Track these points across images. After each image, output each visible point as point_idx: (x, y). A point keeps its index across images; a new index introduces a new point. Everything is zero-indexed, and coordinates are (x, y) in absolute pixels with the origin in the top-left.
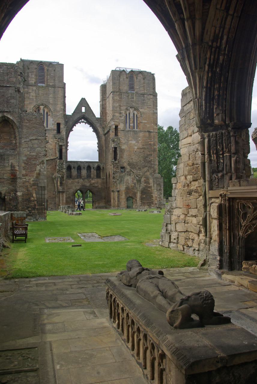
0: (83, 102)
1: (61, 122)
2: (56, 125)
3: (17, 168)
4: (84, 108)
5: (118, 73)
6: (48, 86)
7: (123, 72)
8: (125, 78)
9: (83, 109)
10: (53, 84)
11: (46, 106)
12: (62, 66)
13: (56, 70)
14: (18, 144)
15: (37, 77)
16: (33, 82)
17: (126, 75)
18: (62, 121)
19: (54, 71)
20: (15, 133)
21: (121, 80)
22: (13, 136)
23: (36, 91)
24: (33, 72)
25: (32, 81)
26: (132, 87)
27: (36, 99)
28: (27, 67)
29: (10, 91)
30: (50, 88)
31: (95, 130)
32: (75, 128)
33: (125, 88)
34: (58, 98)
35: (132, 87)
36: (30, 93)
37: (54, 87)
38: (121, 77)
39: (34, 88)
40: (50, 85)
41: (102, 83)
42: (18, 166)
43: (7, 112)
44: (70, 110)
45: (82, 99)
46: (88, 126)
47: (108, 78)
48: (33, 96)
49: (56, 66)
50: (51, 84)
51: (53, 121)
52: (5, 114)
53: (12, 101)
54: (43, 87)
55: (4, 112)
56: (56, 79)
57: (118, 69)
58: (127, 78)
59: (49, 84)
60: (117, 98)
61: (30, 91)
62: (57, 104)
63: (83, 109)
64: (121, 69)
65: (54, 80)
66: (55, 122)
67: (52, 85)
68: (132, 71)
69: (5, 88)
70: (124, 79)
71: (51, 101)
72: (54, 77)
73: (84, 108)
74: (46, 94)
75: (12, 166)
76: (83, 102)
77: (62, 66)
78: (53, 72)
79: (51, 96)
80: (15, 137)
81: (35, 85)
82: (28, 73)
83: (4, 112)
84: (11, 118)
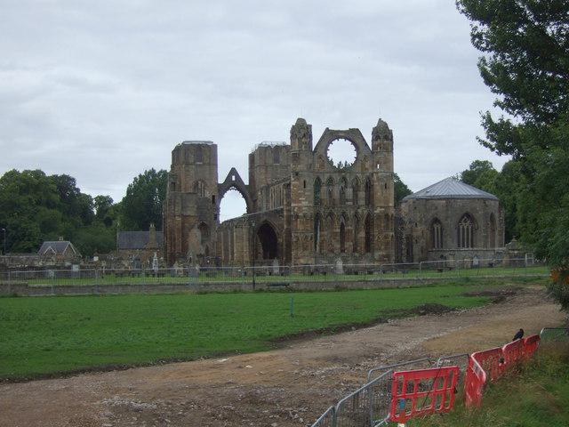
0: (233, 171)
6: (204, 164)
9: (234, 178)
11: (203, 181)
12: (216, 145)
26: (276, 160)
31: (244, 196)
32: (226, 195)
33: (270, 161)
35: (276, 160)
37: (209, 164)
44: (221, 180)
46: (237, 192)
60: (263, 171)
63: (234, 178)
68: (277, 147)
76: (233, 171)
77: (216, 145)
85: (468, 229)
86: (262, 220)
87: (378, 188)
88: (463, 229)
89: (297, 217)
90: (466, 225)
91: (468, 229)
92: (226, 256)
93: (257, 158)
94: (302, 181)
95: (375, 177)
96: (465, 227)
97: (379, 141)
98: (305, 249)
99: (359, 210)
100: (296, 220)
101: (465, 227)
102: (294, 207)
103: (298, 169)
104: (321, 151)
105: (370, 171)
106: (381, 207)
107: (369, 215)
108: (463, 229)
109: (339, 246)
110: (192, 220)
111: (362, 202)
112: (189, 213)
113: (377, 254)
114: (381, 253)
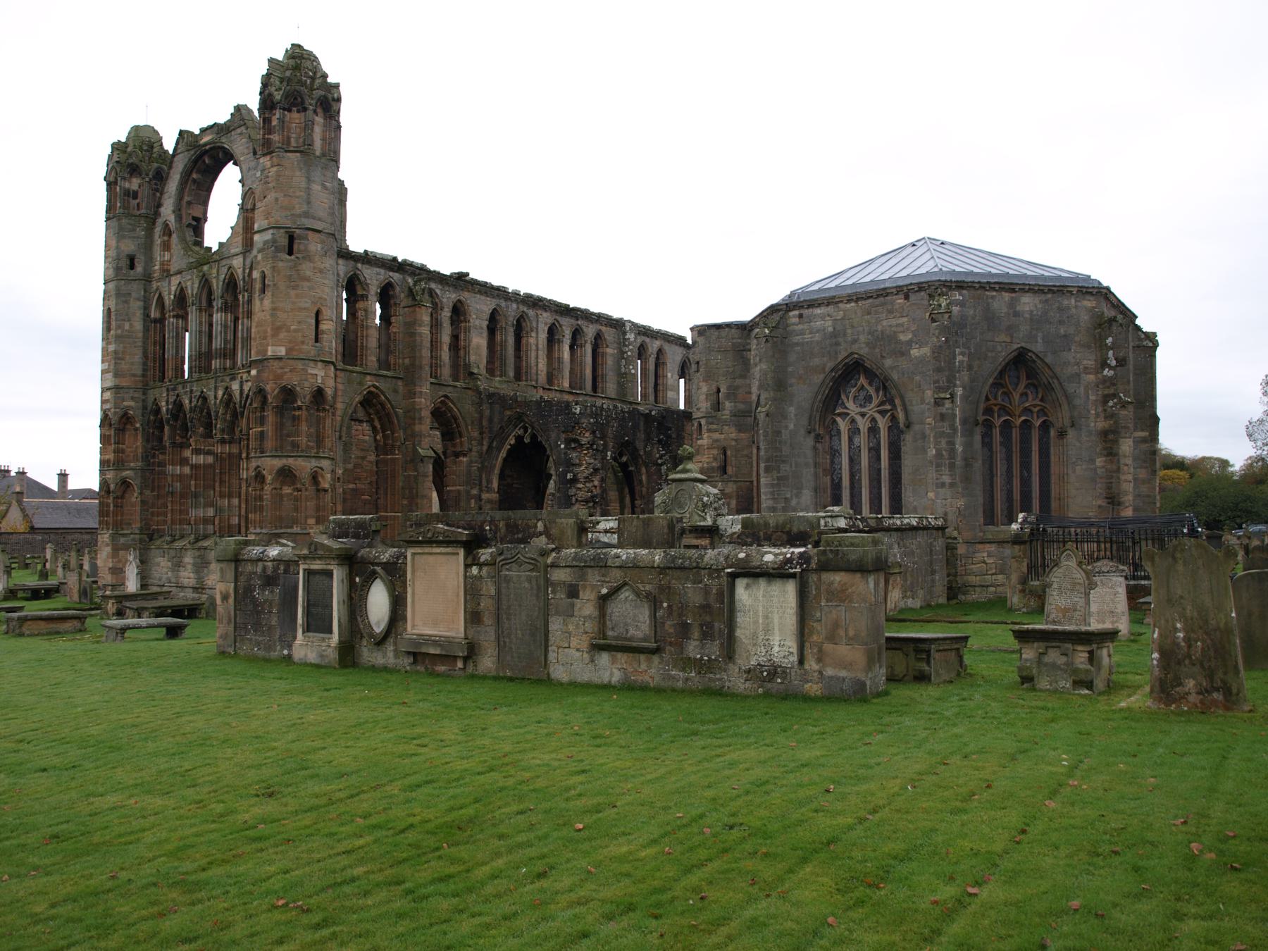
85: (873, 430)
91: (873, 430)
96: (863, 424)
99: (235, 386)
101: (863, 424)
108: (854, 431)
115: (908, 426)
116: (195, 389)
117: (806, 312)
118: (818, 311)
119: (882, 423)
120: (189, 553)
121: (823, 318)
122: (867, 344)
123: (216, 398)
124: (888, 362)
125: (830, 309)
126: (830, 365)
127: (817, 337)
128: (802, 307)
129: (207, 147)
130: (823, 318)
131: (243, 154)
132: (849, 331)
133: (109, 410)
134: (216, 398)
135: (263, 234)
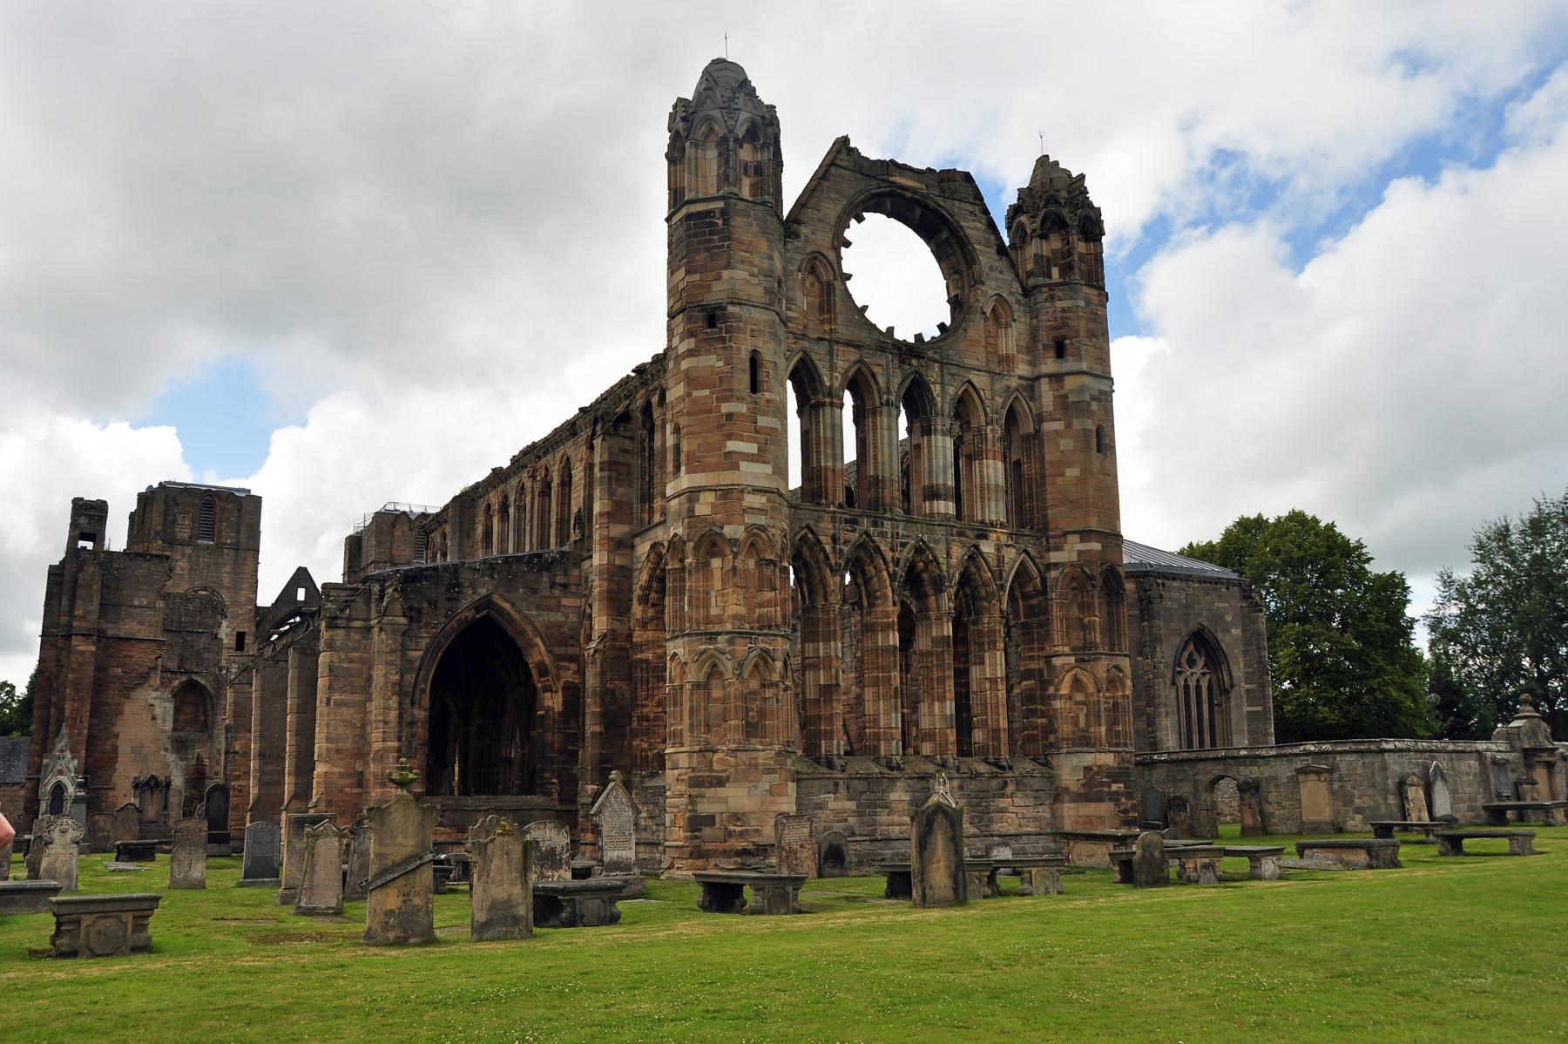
1: (247, 630)
2: (235, 638)
3: (207, 762)
4: (303, 590)
5: (391, 519)
6: (220, 547)
7: (404, 517)
8: (406, 529)
9: (301, 594)
10: (234, 541)
12: (258, 500)
13: (243, 510)
14: (210, 723)
15: (197, 525)
16: (186, 536)
17: (410, 523)
18: (248, 628)
19: (239, 510)
20: (205, 705)
21: (397, 533)
22: (201, 709)
23: (190, 557)
24: (187, 513)
25: (183, 533)
27: (190, 574)
28: (174, 501)
29: (203, 639)
30: (226, 551)
34: (244, 573)
36: (177, 561)
38: (397, 526)
39: (188, 550)
40: (225, 544)
41: (351, 532)
42: (209, 758)
43: (196, 673)
45: (300, 569)
47: (367, 523)
48: (182, 569)
49: (244, 501)
50: (229, 541)
51: (228, 627)
52: (194, 677)
53: (206, 655)
54: (208, 547)
55: (192, 672)
56: (243, 529)
57: (391, 507)
58: (411, 530)
59: (223, 540)
61: (178, 558)
62: (242, 589)
63: (301, 594)
64: (398, 508)
65: (238, 532)
66: (233, 630)
67: (231, 544)
69: (195, 635)
70: (403, 532)
71: (226, 581)
72: (238, 524)
73: (303, 590)
74: (217, 564)
75: (200, 759)
77: (258, 500)
78: (235, 512)
79: (227, 569)
80: (205, 711)
81: (189, 542)
82: (174, 515)
83: (192, 672)
84: (203, 682)
85: (1198, 687)
86: (468, 599)
87: (1066, 444)
88: (1186, 687)
89: (711, 544)
90: (1197, 673)
91: (1198, 687)
92: (270, 782)
93: (370, 552)
94: (745, 355)
95: (1046, 392)
96: (1192, 684)
97: (1055, 243)
98: (752, 729)
99: (987, 548)
100: (705, 566)
101: (1192, 684)
102: (693, 494)
103: (717, 293)
104: (813, 235)
105: (1023, 369)
106: (1086, 535)
107: (1022, 574)
108: (1186, 687)
109: (896, 721)
110: (141, 657)
111: (996, 511)
112: (129, 627)
113: (1070, 768)
114: (1089, 759)
115: (1232, 686)
116: (901, 532)
117: (1167, 582)
118: (1176, 584)
119: (1204, 684)
120: (900, 784)
121: (1179, 589)
122: (1208, 618)
123: (948, 554)
124: (1219, 636)
125: (1183, 584)
126: (1184, 631)
127: (1176, 606)
128: (1168, 579)
129: (909, 195)
130: (1179, 589)
131: (980, 243)
132: (1196, 606)
133: (763, 528)
134: (948, 554)
135: (1097, 380)
